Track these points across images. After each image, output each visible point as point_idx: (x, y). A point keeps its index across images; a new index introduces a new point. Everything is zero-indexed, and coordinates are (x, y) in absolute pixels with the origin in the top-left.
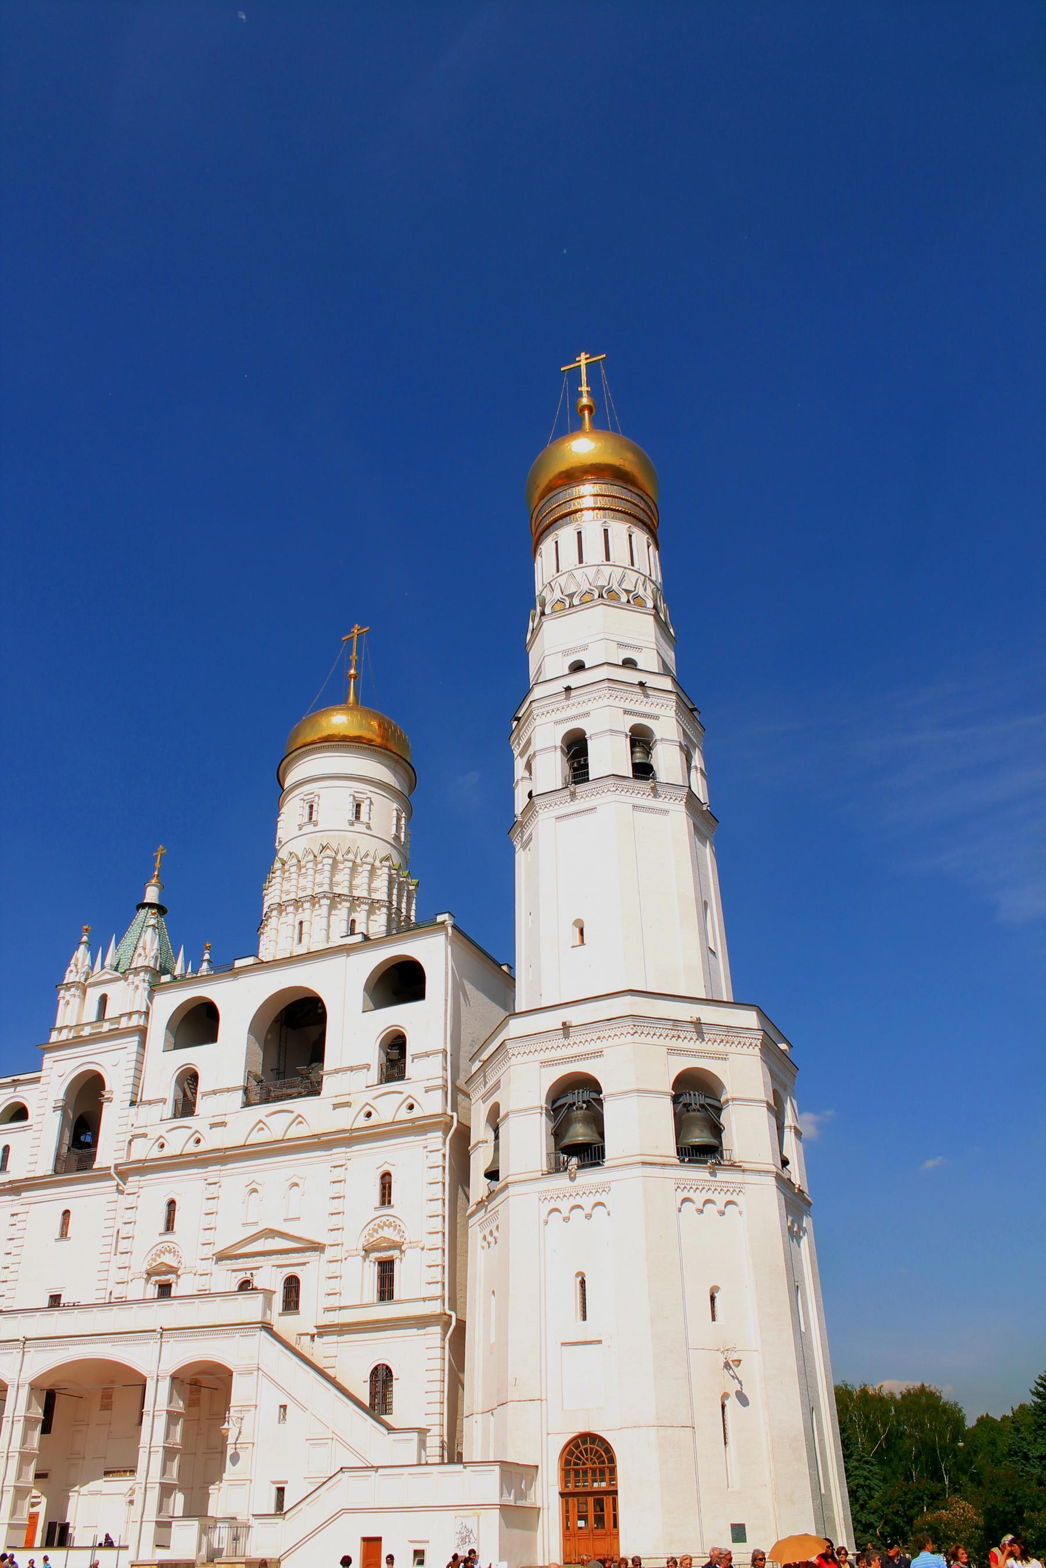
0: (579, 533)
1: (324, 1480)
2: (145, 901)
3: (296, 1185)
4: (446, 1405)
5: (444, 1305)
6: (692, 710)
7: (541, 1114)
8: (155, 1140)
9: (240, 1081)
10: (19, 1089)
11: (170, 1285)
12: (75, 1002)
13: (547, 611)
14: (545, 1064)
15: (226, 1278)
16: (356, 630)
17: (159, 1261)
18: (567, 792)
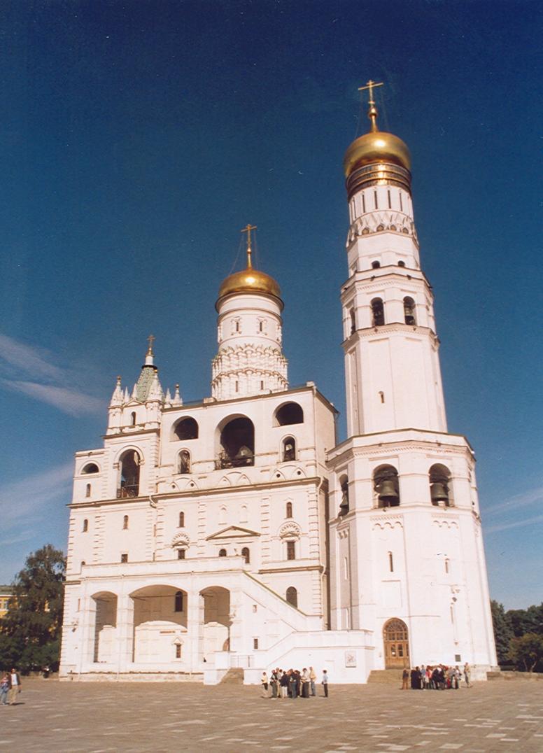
0: (375, 192)
2: (147, 364)
10: (91, 457)
13: (360, 233)
14: (372, 460)
16: (249, 227)
18: (373, 329)
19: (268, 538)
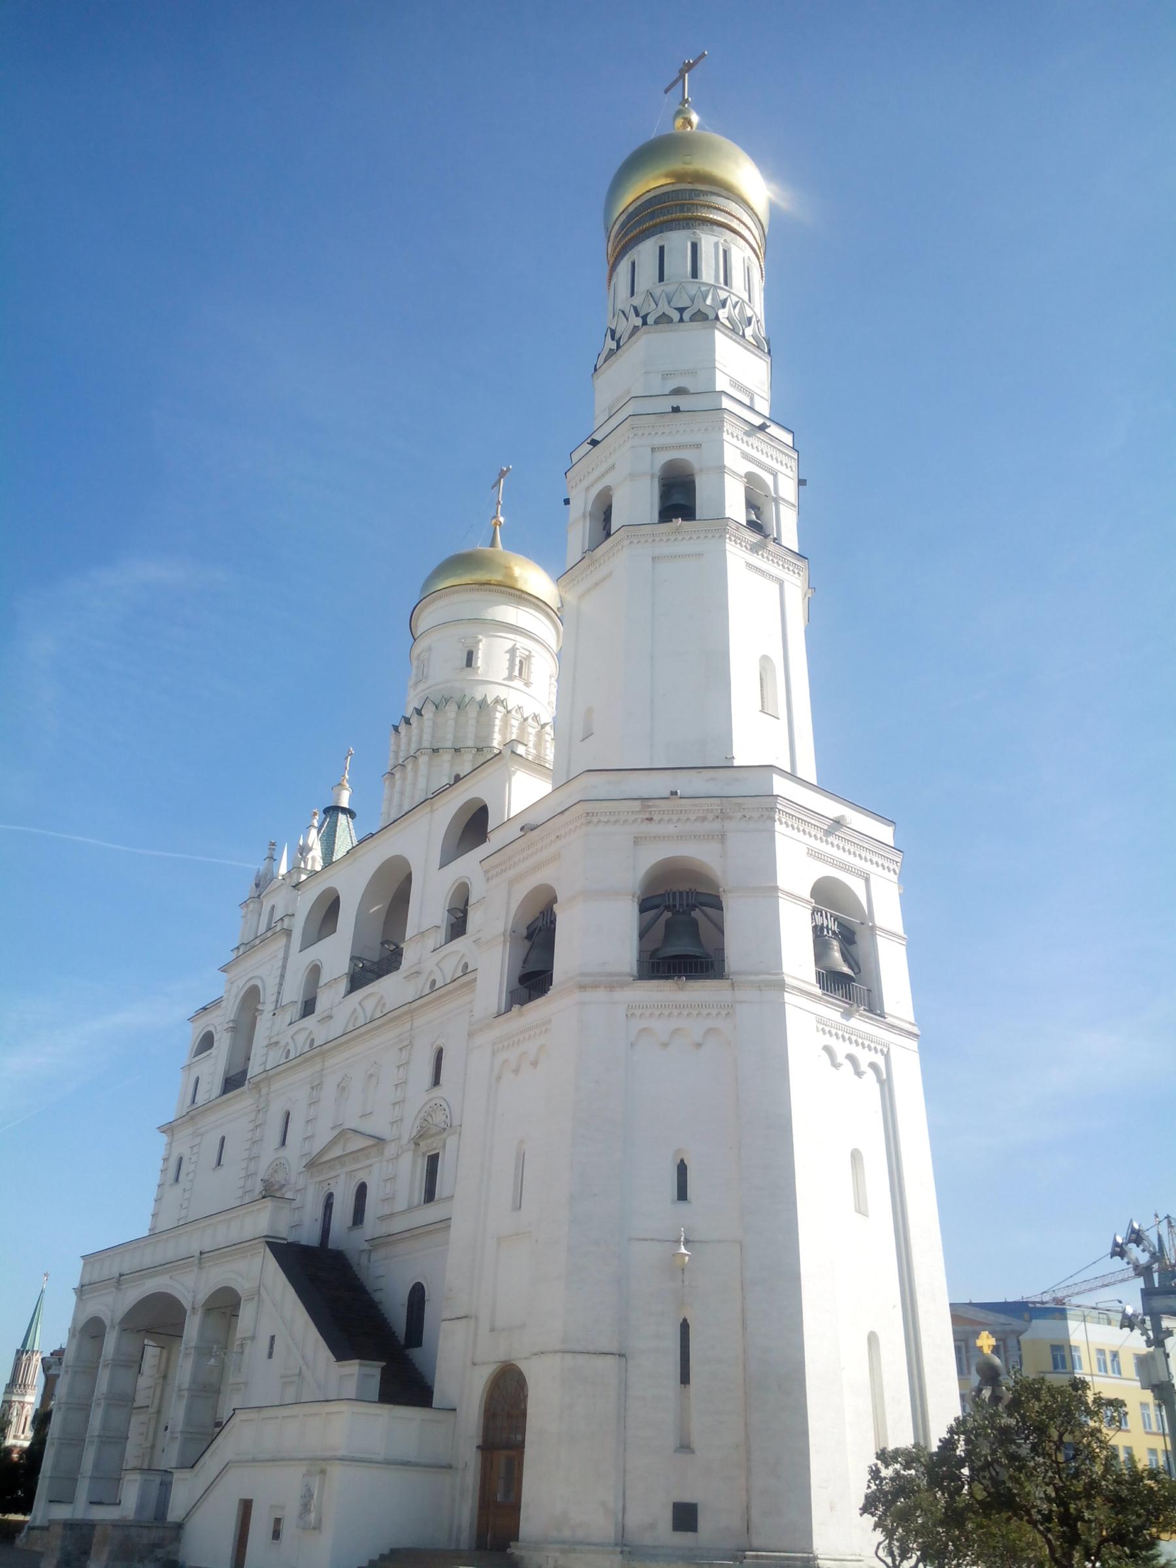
8: (282, 1050)
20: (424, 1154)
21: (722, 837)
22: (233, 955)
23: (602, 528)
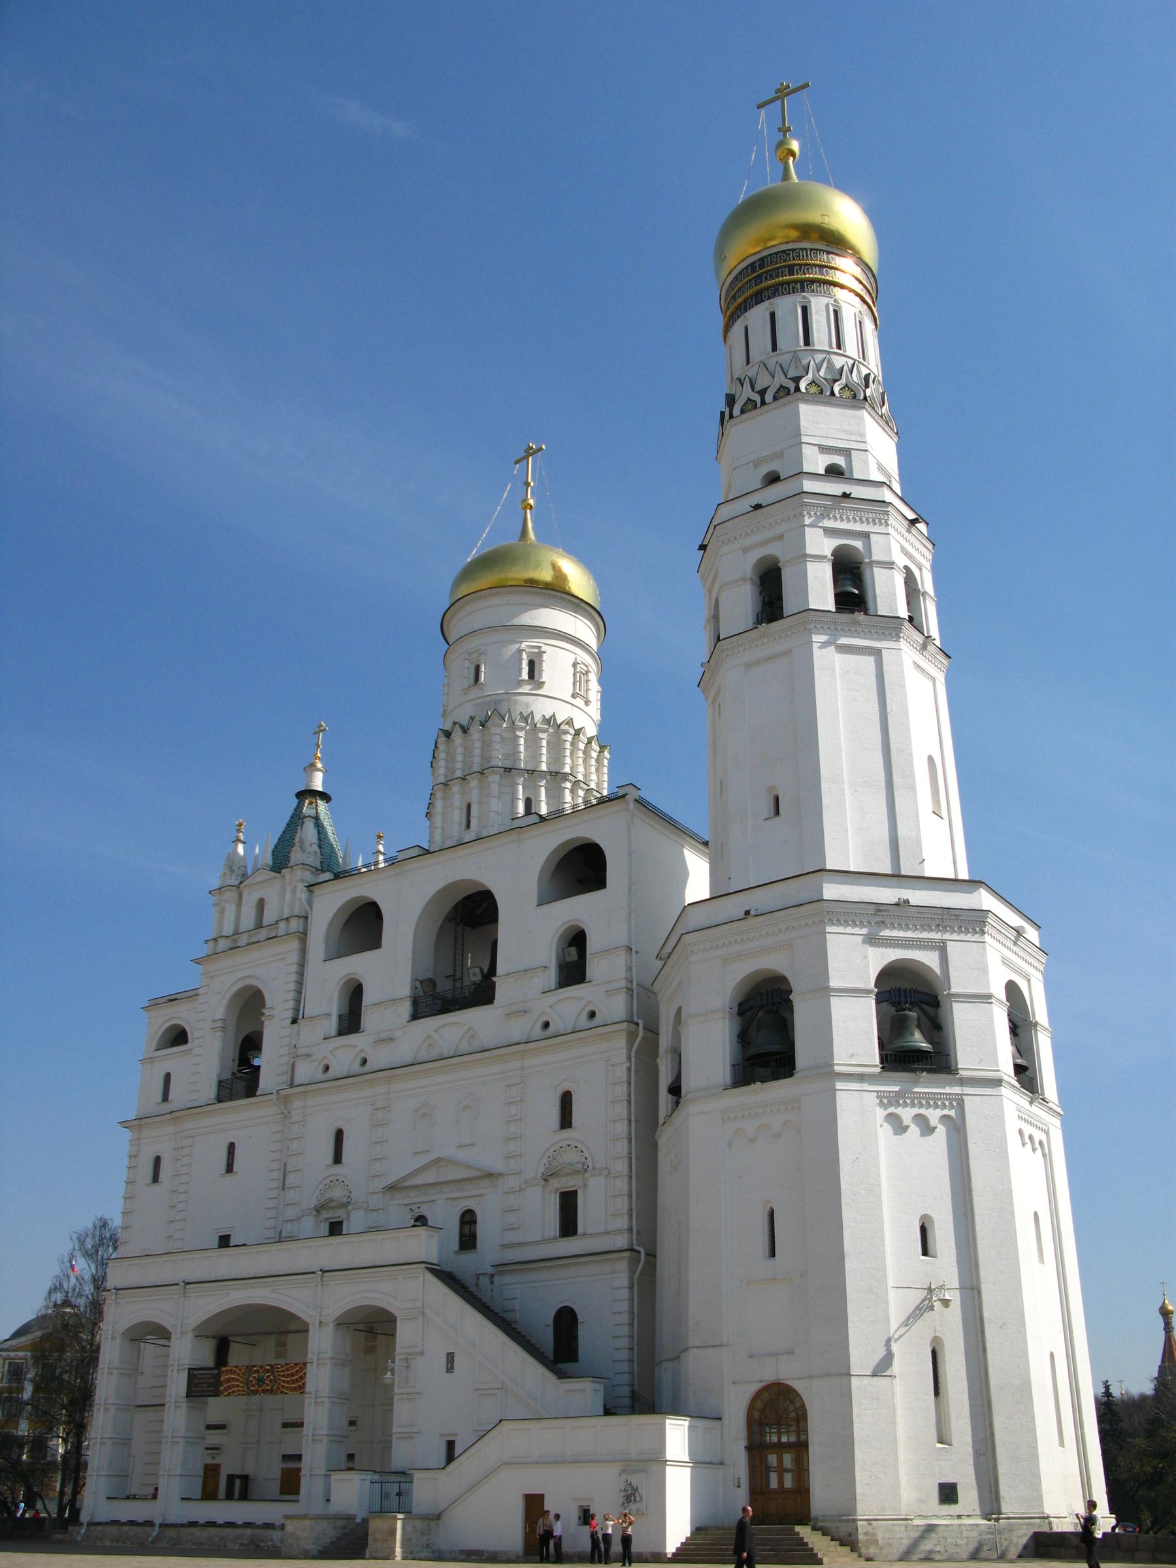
0: (772, 315)
1: (485, 1432)
3: (467, 1107)
4: (635, 1350)
5: (632, 1239)
6: (913, 522)
7: (723, 1018)
9: (405, 989)
11: (341, 1223)
12: (231, 910)
15: (397, 1212)
17: (327, 1197)
19: (512, 1182)
20: (557, 1190)
21: (942, 949)
22: (207, 949)
23: (759, 593)
